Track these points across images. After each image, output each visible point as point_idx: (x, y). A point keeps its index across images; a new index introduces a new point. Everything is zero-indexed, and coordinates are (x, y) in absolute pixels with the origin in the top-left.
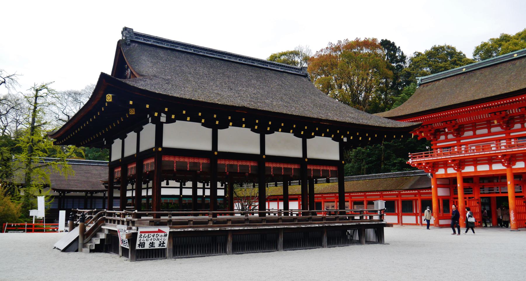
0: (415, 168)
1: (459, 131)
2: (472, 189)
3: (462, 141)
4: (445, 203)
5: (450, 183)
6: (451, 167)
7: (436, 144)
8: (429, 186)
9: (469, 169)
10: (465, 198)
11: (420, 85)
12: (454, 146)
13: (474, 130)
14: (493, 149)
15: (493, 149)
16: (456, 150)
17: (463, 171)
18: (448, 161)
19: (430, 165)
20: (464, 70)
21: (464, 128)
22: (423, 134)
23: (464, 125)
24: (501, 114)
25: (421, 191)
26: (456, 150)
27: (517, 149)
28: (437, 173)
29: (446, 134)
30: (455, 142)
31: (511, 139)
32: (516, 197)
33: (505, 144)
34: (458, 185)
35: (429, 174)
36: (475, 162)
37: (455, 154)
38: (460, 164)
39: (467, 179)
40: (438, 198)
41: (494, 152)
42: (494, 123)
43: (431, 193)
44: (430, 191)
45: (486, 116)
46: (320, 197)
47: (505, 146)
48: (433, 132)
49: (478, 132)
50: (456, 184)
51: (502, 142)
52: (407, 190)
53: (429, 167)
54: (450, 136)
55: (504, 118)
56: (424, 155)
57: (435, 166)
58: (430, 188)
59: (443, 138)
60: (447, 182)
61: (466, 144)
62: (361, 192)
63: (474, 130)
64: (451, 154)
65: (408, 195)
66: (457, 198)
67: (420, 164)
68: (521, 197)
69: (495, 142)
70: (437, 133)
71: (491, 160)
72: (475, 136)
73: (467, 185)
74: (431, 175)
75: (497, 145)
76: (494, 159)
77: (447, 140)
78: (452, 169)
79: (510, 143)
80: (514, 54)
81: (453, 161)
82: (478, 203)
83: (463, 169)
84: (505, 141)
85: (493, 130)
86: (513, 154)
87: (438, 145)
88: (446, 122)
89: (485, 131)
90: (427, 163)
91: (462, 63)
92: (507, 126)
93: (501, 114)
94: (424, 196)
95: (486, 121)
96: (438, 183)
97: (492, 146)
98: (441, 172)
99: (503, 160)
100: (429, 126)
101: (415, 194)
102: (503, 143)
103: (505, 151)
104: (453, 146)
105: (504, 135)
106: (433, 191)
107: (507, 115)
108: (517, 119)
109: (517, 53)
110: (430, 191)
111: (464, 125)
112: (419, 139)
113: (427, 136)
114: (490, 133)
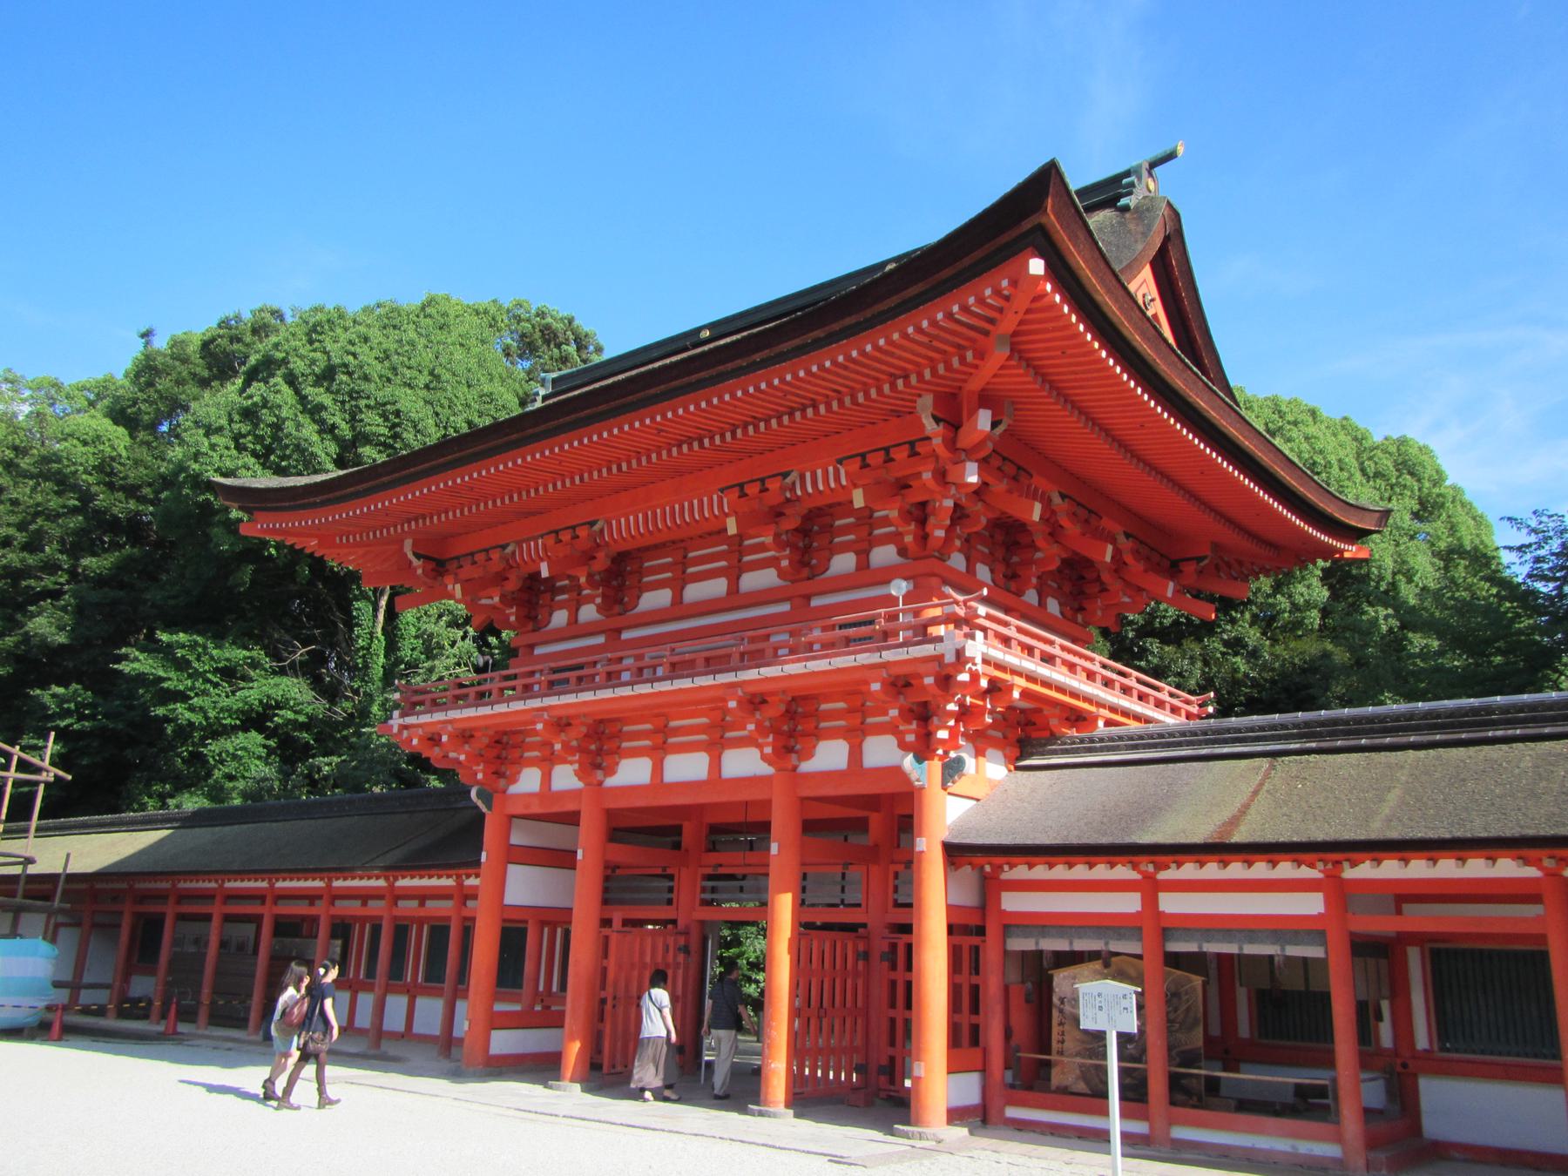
2: (671, 877)
7: (532, 647)
10: (606, 922)
17: (611, 782)
21: (641, 572)
38: (599, 742)
49: (694, 592)
55: (777, 514)
57: (504, 749)
59: (560, 618)
67: (434, 740)
72: (680, 608)
73: (622, 853)
77: (575, 630)
81: (561, 724)
83: (611, 771)
85: (751, 581)
87: (538, 651)
89: (718, 587)
90: (465, 735)
96: (516, 839)
98: (529, 781)
100: (495, 555)
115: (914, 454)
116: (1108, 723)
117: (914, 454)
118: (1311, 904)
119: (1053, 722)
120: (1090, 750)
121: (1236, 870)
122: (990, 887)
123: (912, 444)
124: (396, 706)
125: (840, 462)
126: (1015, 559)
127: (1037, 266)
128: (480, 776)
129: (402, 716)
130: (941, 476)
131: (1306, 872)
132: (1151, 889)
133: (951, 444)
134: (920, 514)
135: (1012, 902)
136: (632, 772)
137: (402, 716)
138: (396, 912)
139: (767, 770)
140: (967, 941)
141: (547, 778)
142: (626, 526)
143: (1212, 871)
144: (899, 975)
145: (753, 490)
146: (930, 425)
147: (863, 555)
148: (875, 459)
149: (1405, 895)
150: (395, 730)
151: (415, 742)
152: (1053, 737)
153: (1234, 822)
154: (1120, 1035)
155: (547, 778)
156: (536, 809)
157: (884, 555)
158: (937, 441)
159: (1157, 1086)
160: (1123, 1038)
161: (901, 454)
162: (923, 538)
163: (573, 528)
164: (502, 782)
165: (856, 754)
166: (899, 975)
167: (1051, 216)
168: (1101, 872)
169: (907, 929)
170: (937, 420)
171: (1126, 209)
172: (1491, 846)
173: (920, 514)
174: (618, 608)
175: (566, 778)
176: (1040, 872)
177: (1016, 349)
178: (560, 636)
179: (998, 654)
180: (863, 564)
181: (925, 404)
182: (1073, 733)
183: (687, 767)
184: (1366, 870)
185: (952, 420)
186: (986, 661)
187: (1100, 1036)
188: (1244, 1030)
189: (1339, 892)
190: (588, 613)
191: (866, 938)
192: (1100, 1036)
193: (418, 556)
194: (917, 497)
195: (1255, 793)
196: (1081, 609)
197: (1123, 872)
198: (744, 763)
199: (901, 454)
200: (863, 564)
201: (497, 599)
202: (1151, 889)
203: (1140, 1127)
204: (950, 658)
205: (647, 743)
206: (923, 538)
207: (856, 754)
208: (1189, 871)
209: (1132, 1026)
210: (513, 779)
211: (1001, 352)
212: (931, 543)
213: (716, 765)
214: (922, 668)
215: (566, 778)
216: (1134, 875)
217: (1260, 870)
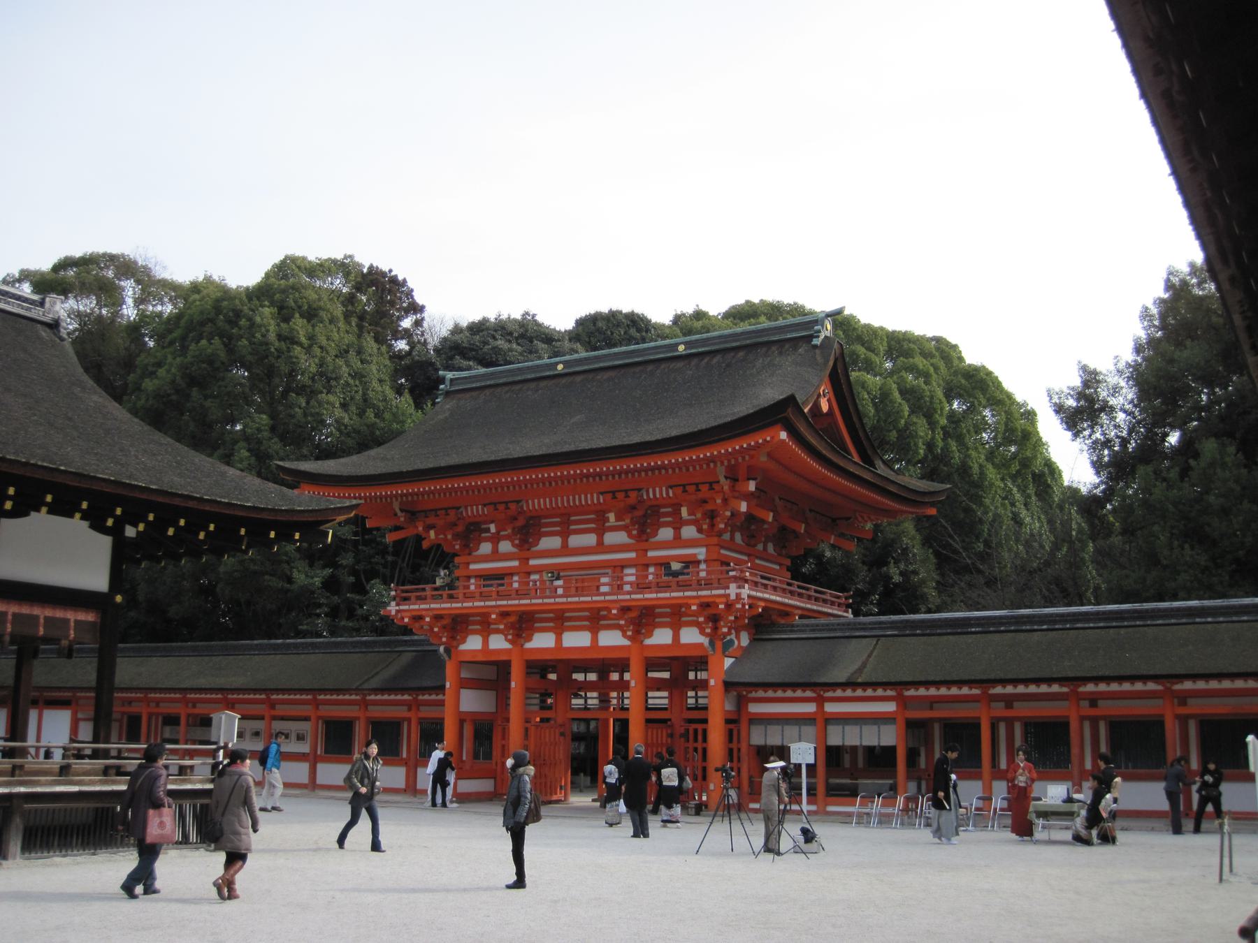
0: (406, 630)
1: (527, 532)
3: (532, 562)
4: (484, 733)
5: (494, 675)
6: (498, 631)
8: (439, 684)
9: (542, 641)
11: (448, 394)
12: (512, 575)
13: (565, 534)
14: (604, 589)
15: (604, 589)
16: (516, 585)
17: (528, 645)
18: (489, 614)
19: (445, 622)
20: (560, 367)
22: (432, 533)
23: (540, 517)
24: (627, 496)
25: (322, 697)
26: (516, 585)
27: (654, 596)
28: (463, 647)
29: (495, 540)
30: (516, 563)
31: (647, 566)
32: (648, 721)
33: (633, 579)
34: (513, 684)
35: (442, 649)
36: (560, 621)
37: (507, 596)
38: (522, 625)
39: (538, 667)
40: (462, 719)
41: (628, 597)
42: (488, 530)
43: (441, 703)
44: (440, 697)
45: (594, 499)
46: (138, 700)
47: (631, 583)
48: (460, 528)
49: (575, 541)
50: (509, 682)
51: (627, 571)
52: (382, 690)
53: (444, 627)
54: (505, 546)
55: (633, 508)
56: (428, 593)
57: (458, 625)
58: (441, 689)
59: (486, 548)
60: (490, 673)
61: (539, 570)
62: (255, 691)
63: (565, 534)
64: (500, 596)
65: (389, 707)
66: (508, 720)
67: (418, 618)
68: (664, 721)
69: (609, 571)
70: (471, 533)
71: (595, 620)
72: (565, 550)
74: (447, 651)
75: (613, 577)
76: (604, 618)
77: (495, 555)
78: (501, 637)
79: (468, 587)
80: (557, 363)
81: (504, 614)
82: (562, 734)
83: (529, 639)
84: (633, 571)
85: (611, 538)
86: (646, 607)
87: (472, 567)
88: (495, 504)
89: (590, 540)
90: (437, 617)
91: (465, 363)
92: (642, 532)
93: (627, 496)
94: (426, 712)
95: (596, 512)
96: (463, 675)
97: (604, 580)
98: (473, 643)
99: (622, 622)
100: (452, 513)
101: (409, 705)
102: (630, 575)
103: (564, 600)
104: (509, 573)
105: (633, 555)
106: (448, 697)
107: (641, 502)
108: (666, 515)
109: (685, 343)
110: (440, 697)
111: (540, 517)
112: (425, 545)
113: (446, 539)
114: (601, 547)
115: (711, 489)
116: (801, 617)
117: (711, 489)
118: (890, 707)
119: (774, 617)
120: (792, 631)
121: (859, 692)
122: (742, 702)
123: (711, 484)
124: (394, 599)
125: (671, 487)
126: (753, 527)
127: (783, 435)
128: (444, 639)
129: (398, 605)
130: (725, 500)
131: (890, 693)
132: (820, 701)
133: (732, 488)
134: (712, 516)
135: (754, 708)
136: (542, 641)
137: (398, 605)
138: (368, 714)
139: (626, 642)
140: (731, 726)
141: (486, 642)
142: (536, 504)
143: (849, 693)
144: (699, 745)
145: (620, 495)
146: (722, 480)
147: (677, 530)
148: (691, 489)
149: (932, 702)
150: (393, 613)
151: (406, 620)
152: (773, 624)
153: (860, 670)
154: (808, 765)
155: (486, 642)
156: (480, 658)
157: (689, 532)
158: (726, 488)
159: (821, 790)
160: (808, 765)
161: (704, 488)
162: (712, 526)
163: (506, 503)
164: (455, 643)
165: (676, 637)
166: (699, 745)
167: (790, 413)
168: (799, 693)
169: (705, 721)
170: (726, 478)
171: (815, 347)
172: (960, 683)
173: (712, 516)
174: (526, 546)
175: (498, 643)
176: (770, 694)
177: (769, 455)
178: (485, 559)
179: (754, 593)
180: (677, 536)
181: (721, 472)
182: (783, 622)
183: (577, 640)
184: (911, 692)
185: (733, 478)
186: (749, 596)
187: (800, 765)
188: (861, 763)
189: (902, 701)
190: (505, 546)
191: (672, 726)
192: (800, 765)
193: (402, 510)
194: (709, 507)
195: (869, 656)
196: (784, 547)
197: (809, 694)
198: (611, 639)
199: (704, 488)
200: (677, 536)
201: (449, 537)
202: (820, 701)
203: (813, 808)
204: (733, 597)
205: (551, 624)
206: (712, 526)
207: (676, 637)
208: (839, 693)
209: (812, 761)
210: (463, 641)
211: (764, 459)
212: (716, 529)
213: (595, 639)
214: (718, 600)
215: (498, 643)
216: (814, 695)
217: (870, 692)
